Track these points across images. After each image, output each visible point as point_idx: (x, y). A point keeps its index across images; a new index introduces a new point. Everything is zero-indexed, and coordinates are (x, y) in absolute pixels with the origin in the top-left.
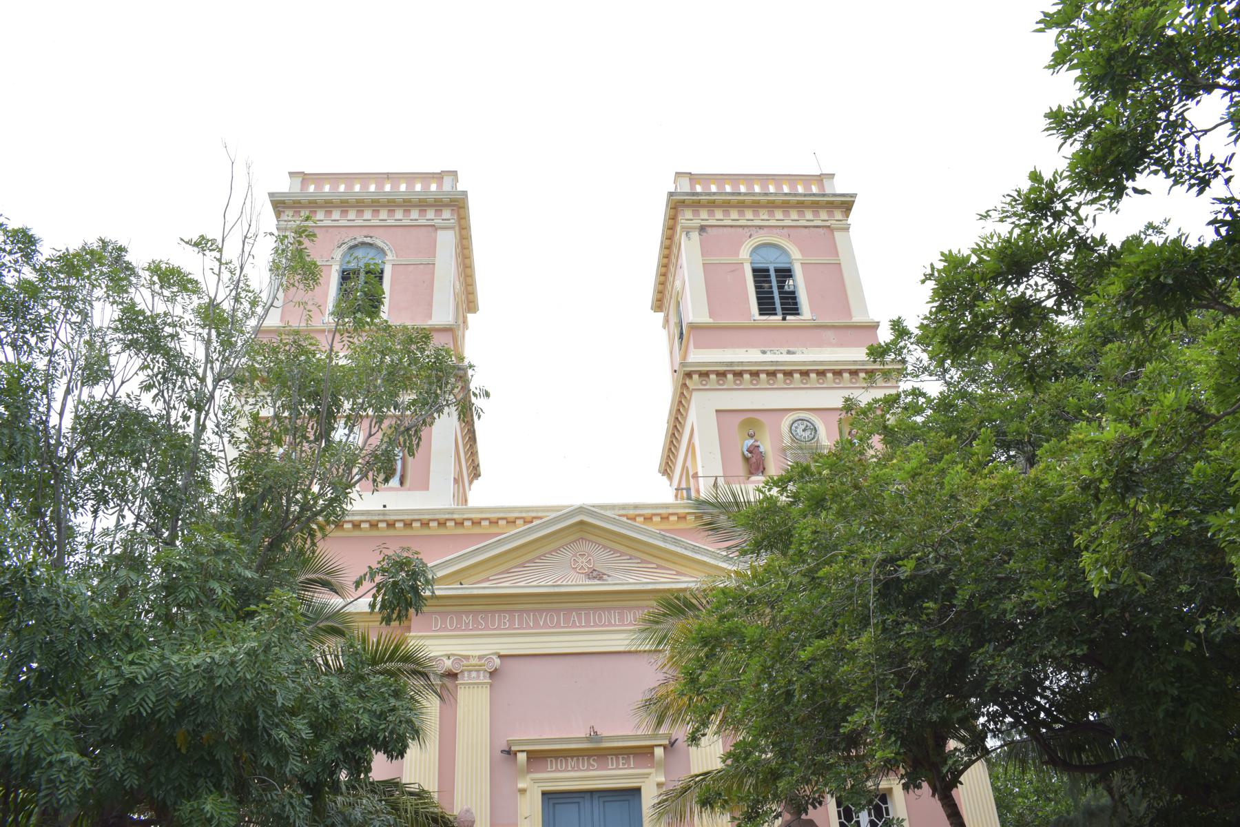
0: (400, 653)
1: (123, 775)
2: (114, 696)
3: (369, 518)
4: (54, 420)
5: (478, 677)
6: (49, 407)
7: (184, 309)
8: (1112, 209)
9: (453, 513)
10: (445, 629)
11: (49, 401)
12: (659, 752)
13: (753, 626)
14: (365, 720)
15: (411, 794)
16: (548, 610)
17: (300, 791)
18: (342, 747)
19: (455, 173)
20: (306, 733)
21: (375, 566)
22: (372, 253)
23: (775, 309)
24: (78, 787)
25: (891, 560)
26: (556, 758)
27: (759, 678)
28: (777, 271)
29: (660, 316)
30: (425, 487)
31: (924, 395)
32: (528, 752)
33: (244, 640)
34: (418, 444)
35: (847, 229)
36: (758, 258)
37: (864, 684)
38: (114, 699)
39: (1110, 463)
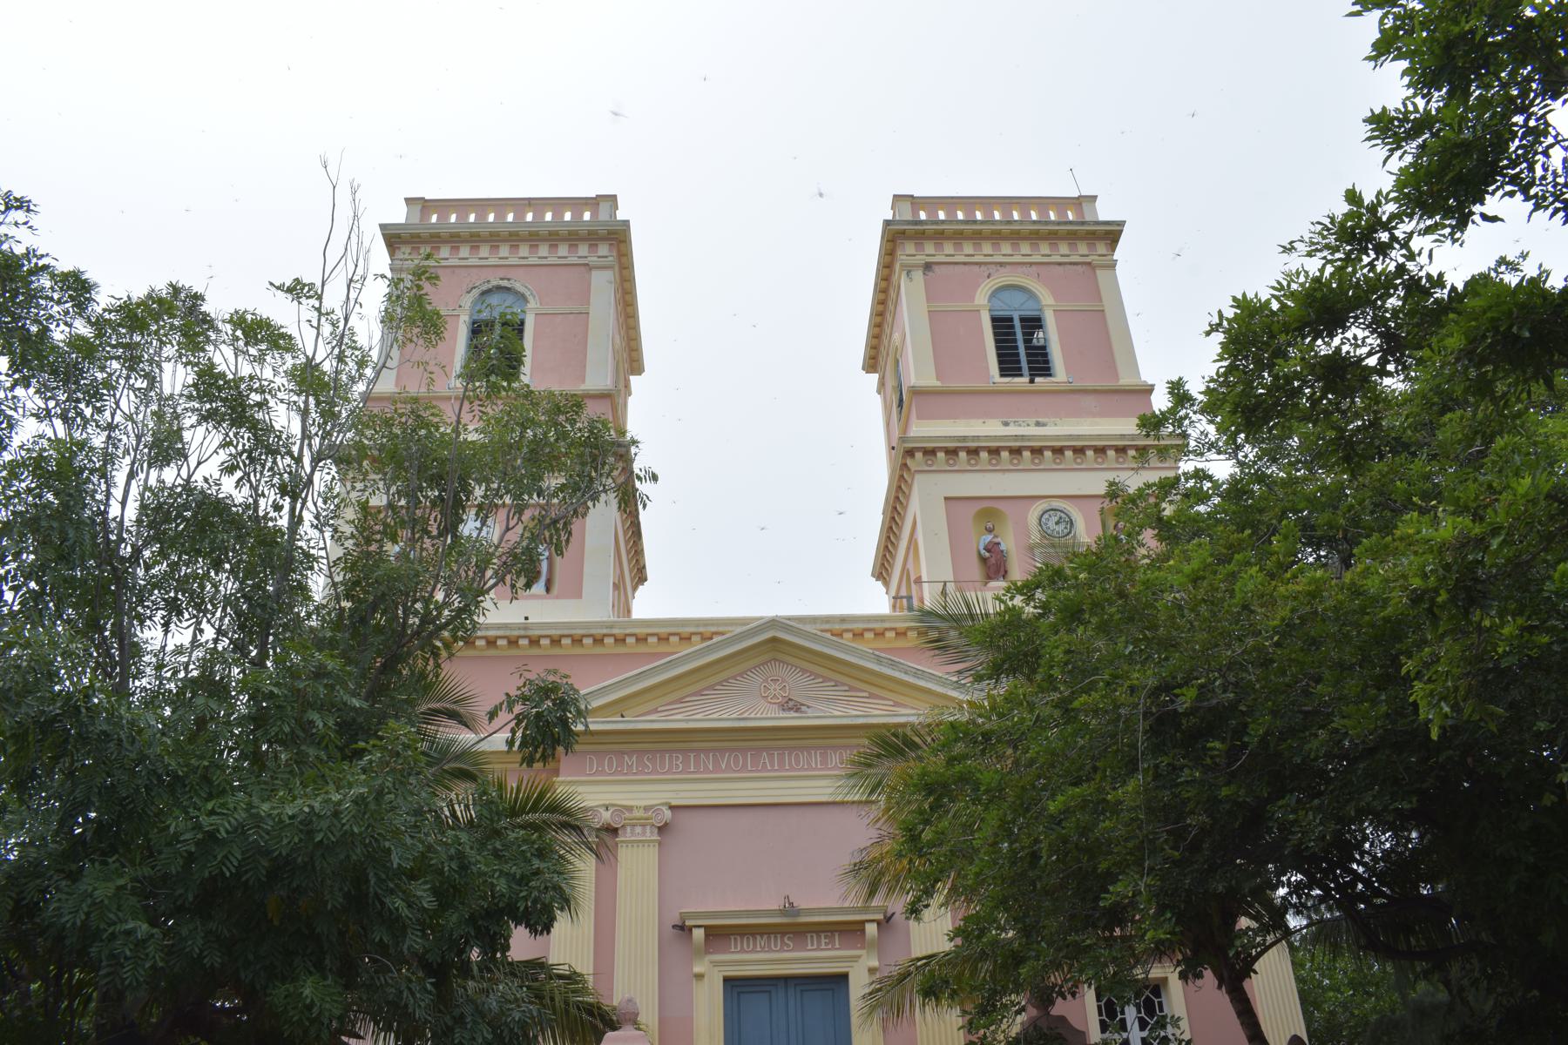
0: (545, 803)
1: (201, 951)
2: (190, 853)
3: (508, 633)
4: (114, 511)
5: (644, 833)
6: (108, 494)
7: (274, 371)
8: (1454, 241)
10: (602, 773)
11: (109, 487)
12: (871, 929)
13: (989, 770)
14: (502, 886)
15: (560, 977)
16: (732, 750)
17: (421, 974)
18: (472, 919)
19: (613, 198)
20: (428, 902)
21: (514, 693)
22: (510, 299)
23: (1020, 369)
24: (147, 965)
25: (1166, 687)
26: (742, 935)
27: (996, 835)
28: (1022, 320)
29: (875, 377)
31: (1209, 478)
32: (706, 927)
33: (350, 786)
34: (568, 541)
35: (1112, 265)
36: (998, 304)
37: (1130, 845)
38: (190, 858)
39: (1447, 567)
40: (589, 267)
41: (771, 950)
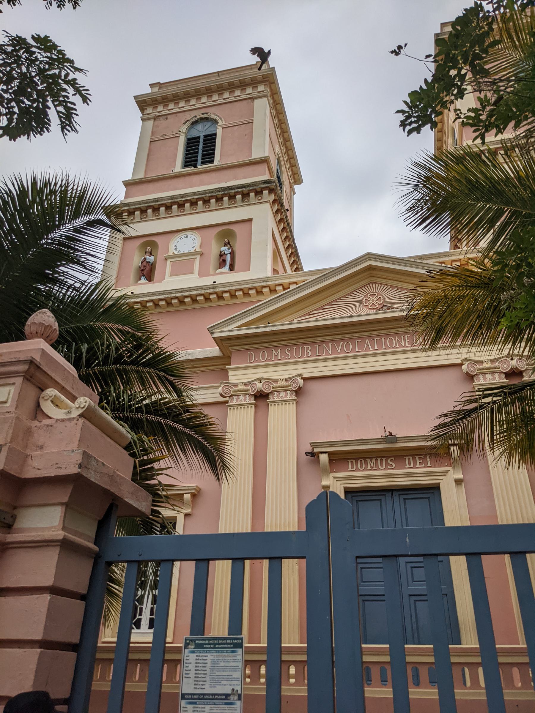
3: (203, 292)
9: (267, 281)
10: (259, 361)
16: (343, 340)
22: (209, 124)
26: (357, 459)
30: (248, 268)
32: (330, 454)
40: (253, 99)
41: (378, 469)
